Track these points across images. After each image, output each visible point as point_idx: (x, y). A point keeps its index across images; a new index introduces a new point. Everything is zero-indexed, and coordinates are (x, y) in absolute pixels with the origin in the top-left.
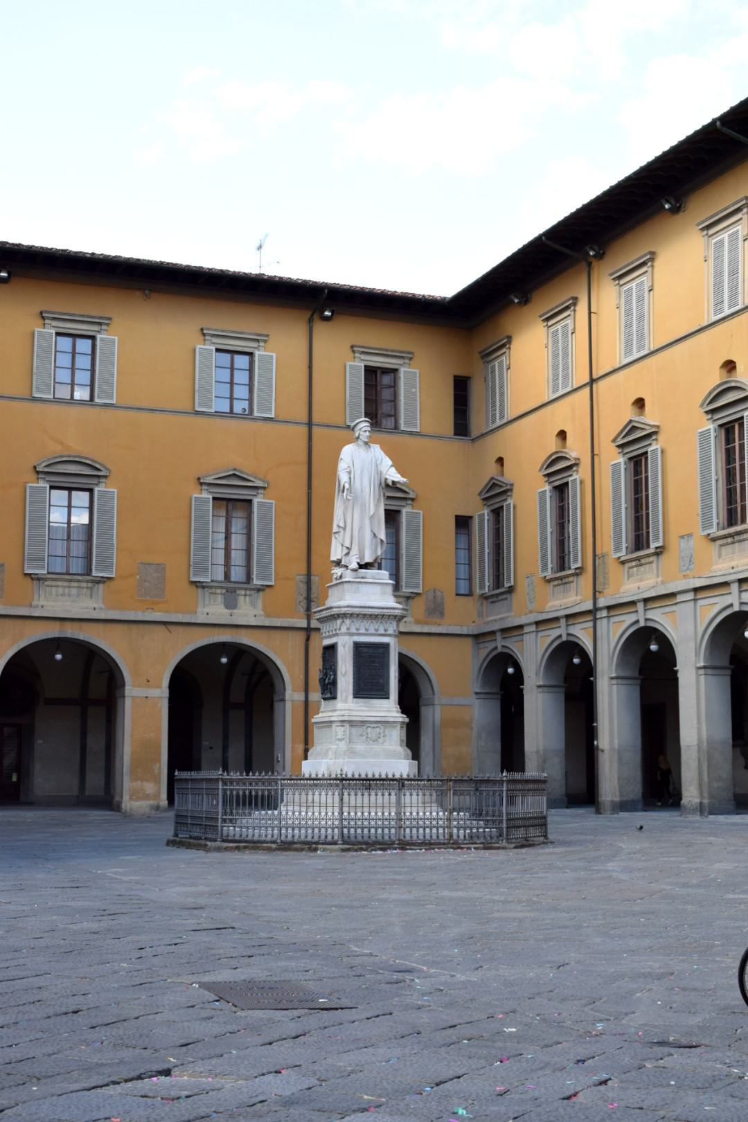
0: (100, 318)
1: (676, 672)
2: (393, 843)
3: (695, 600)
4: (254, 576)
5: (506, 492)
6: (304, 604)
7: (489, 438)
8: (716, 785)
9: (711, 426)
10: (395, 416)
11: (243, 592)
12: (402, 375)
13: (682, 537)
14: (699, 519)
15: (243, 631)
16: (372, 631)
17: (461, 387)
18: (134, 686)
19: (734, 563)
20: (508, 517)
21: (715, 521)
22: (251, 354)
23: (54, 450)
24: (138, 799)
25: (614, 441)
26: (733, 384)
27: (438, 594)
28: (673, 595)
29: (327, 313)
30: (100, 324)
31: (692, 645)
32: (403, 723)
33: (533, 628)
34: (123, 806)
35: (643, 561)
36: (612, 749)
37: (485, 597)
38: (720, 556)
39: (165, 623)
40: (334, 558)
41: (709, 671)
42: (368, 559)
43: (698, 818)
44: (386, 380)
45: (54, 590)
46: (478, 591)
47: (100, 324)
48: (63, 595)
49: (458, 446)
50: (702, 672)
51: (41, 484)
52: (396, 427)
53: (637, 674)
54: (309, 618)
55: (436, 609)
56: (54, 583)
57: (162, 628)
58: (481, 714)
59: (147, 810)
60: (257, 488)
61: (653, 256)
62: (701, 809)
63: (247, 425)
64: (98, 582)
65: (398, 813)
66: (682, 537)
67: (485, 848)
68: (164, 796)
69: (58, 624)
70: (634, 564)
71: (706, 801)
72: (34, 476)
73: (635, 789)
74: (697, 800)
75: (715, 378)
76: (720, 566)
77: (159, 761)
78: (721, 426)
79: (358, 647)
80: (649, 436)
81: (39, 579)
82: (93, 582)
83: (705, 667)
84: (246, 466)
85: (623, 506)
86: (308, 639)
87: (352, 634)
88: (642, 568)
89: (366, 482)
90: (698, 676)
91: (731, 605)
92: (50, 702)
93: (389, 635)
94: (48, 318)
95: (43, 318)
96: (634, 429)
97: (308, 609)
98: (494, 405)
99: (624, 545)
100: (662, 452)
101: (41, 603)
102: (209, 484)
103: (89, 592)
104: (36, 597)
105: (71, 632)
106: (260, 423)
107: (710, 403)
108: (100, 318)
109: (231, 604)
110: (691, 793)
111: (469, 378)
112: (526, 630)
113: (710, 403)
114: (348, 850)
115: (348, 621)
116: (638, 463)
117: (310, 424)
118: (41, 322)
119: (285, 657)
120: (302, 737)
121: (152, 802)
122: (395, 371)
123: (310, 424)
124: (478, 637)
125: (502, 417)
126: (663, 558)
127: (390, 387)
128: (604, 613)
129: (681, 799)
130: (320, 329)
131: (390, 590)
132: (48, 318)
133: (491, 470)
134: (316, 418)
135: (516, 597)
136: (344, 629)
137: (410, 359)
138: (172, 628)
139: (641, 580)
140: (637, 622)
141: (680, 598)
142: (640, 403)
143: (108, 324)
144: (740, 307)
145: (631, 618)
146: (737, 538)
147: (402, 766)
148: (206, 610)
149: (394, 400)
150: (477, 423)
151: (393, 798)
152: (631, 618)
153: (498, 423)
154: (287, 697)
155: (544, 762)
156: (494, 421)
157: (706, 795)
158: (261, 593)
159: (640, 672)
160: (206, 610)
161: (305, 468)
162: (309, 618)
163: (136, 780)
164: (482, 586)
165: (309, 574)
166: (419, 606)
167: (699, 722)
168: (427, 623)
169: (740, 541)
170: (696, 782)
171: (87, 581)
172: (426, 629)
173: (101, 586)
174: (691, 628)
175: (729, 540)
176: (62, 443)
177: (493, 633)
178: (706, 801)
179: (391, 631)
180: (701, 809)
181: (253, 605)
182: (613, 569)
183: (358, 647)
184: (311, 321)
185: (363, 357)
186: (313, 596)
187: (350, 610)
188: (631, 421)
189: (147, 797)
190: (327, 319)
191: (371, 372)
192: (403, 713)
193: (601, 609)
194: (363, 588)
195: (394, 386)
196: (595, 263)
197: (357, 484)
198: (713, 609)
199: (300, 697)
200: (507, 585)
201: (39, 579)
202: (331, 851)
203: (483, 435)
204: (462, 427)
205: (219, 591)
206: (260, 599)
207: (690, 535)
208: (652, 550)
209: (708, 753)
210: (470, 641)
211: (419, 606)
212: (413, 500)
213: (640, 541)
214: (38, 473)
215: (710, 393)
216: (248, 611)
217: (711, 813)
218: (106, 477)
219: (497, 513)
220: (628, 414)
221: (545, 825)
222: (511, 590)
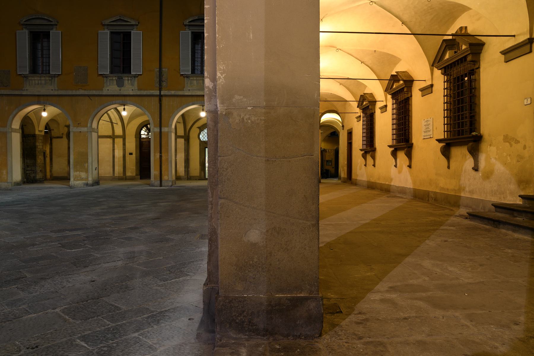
11: (127, 78)
18: (74, 126)
24: (78, 180)
39: (89, 96)
48: (38, 84)
54: (160, 90)
59: (82, 185)
64: (54, 77)
77: (87, 162)
86: (160, 101)
97: (160, 85)
102: (108, 25)
109: (120, 84)
158: (136, 79)
162: (160, 90)
163: (77, 171)
173: (56, 79)
189: (82, 179)
205: (114, 78)
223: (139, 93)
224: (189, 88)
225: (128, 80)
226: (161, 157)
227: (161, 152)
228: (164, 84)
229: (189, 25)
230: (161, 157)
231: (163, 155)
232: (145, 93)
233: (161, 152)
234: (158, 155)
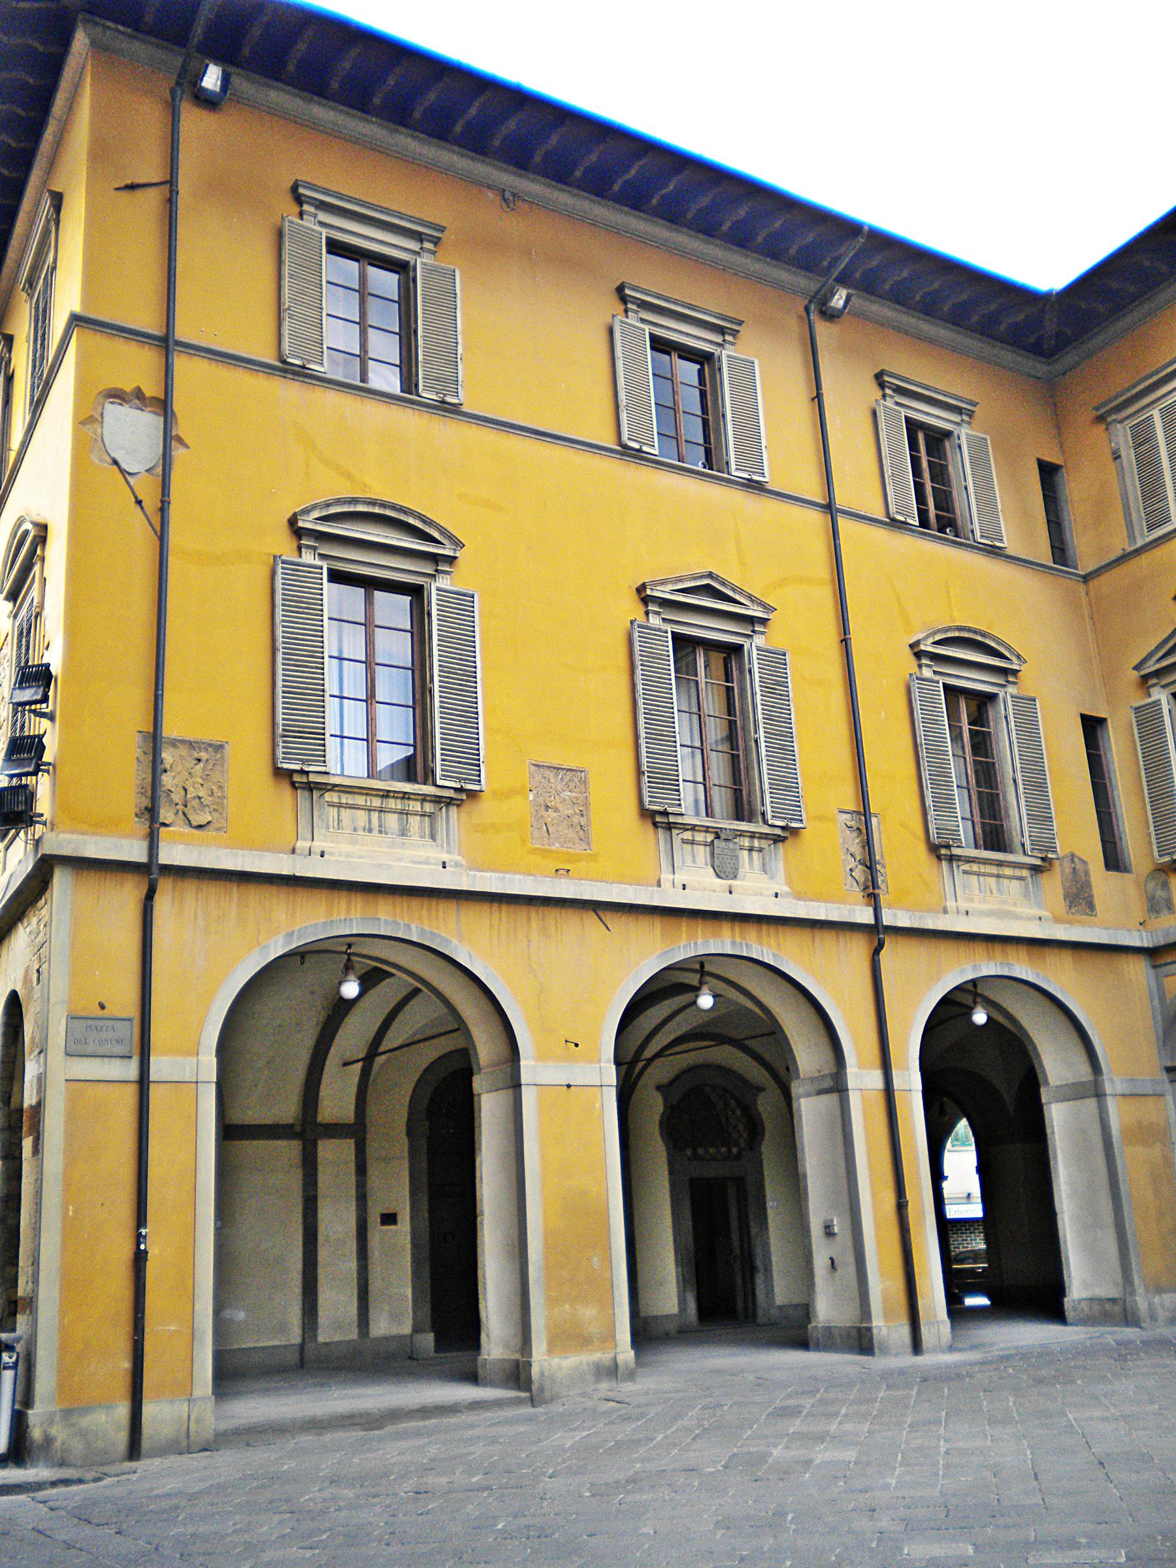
11: (746, 842)
15: (752, 932)
23: (330, 486)
27: (1079, 866)
34: (535, 1371)
51: (308, 558)
55: (1080, 898)
56: (345, 799)
57: (590, 918)
60: (751, 620)
64: (449, 802)
68: (624, 1334)
81: (310, 787)
84: (730, 573)
101: (318, 845)
102: (665, 603)
106: (737, 497)
111: (1060, 467)
118: (296, 209)
121: (597, 1356)
138: (609, 918)
148: (680, 878)
154: (851, 1083)
160: (680, 878)
161: (825, 596)
165: (865, 812)
173: (453, 811)
176: (348, 476)
191: (913, 427)
199: (875, 1079)
205: (700, 837)
211: (1054, 885)
216: (758, 888)
218: (451, 560)
224: (964, 905)
225: (751, 849)
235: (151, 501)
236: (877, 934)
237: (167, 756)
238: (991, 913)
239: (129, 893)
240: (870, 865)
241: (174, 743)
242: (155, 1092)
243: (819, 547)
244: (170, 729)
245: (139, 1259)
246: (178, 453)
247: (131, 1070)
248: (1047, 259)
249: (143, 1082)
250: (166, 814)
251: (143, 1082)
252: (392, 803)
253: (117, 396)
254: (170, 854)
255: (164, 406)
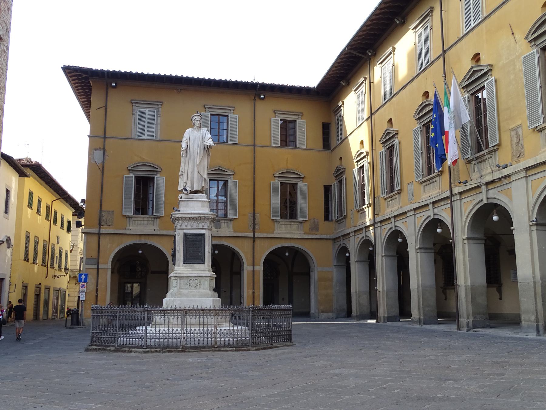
0: (157, 102)
1: (408, 251)
2: (179, 348)
3: (415, 215)
4: (229, 214)
5: (343, 172)
6: (252, 226)
7: (337, 149)
8: (427, 309)
9: (419, 126)
10: (295, 141)
11: (223, 221)
12: (298, 123)
13: (409, 184)
14: (415, 173)
15: (224, 239)
16: (195, 227)
17: (326, 129)
19: (430, 194)
20: (344, 182)
21: (421, 174)
22: (227, 116)
25: (380, 141)
26: (427, 103)
27: (316, 220)
28: (405, 213)
29: (262, 96)
30: (158, 105)
31: (414, 237)
32: (211, 278)
33: (353, 234)
35: (393, 198)
36: (383, 290)
37: (337, 221)
38: (424, 191)
40: (179, 189)
41: (422, 251)
42: (195, 188)
43: (418, 326)
44: (291, 125)
45: (136, 222)
46: (334, 219)
47: (158, 105)
49: (325, 153)
50: (418, 251)
51: (131, 175)
52: (296, 146)
53: (395, 254)
55: (315, 228)
56: (136, 219)
58: (336, 274)
60: (230, 175)
61: (394, 50)
62: (419, 321)
63: (225, 147)
64: (157, 218)
65: (182, 329)
66: (409, 184)
67: (235, 351)
69: (138, 237)
70: (390, 199)
71: (422, 317)
72: (128, 172)
73: (396, 311)
74: (418, 317)
75: (419, 101)
76: (424, 196)
78: (423, 125)
79: (186, 235)
80: (394, 136)
81: (129, 217)
82: (154, 218)
83: (420, 249)
85: (385, 172)
87: (183, 229)
88: (393, 201)
89: (196, 147)
90: (417, 253)
91: (430, 216)
92: (153, 272)
93: (205, 229)
94: (134, 103)
95: (132, 103)
96: (388, 133)
97: (254, 228)
98: (338, 134)
99: (385, 191)
100: (399, 143)
101: (130, 228)
103: (152, 222)
104: (128, 225)
105: (144, 240)
106: (231, 147)
107: (418, 114)
108: (157, 102)
109: (218, 227)
110: (415, 313)
112: (351, 235)
113: (418, 114)
114: (148, 352)
115: (180, 222)
116: (390, 150)
117: (254, 146)
118: (131, 105)
119: (243, 250)
120: (252, 287)
122: (295, 121)
123: (254, 146)
124: (335, 240)
125: (341, 138)
126: (402, 194)
127: (293, 129)
128: (379, 224)
129: (411, 316)
130: (259, 104)
131: (207, 204)
132: (134, 103)
133: (337, 163)
134: (257, 143)
135: (348, 220)
136: (178, 226)
137: (302, 116)
139: (393, 207)
140: (392, 228)
141: (408, 214)
142: (390, 121)
143: (161, 105)
144: (430, 62)
145: (389, 226)
146: (431, 181)
147: (211, 301)
149: (295, 135)
150: (333, 143)
151: (180, 321)
152: (389, 226)
153: (340, 141)
155: (359, 297)
156: (338, 141)
157: (422, 314)
158: (232, 222)
159: (397, 253)
164: (335, 217)
165: (254, 213)
166: (307, 226)
167: (418, 276)
168: (310, 234)
169: (433, 183)
170: (417, 307)
171: (151, 218)
172: (310, 237)
173: (158, 220)
174: (413, 229)
175: (428, 182)
176: (140, 157)
177: (339, 237)
178: (422, 317)
179: (206, 227)
180: (419, 321)
181: (228, 227)
182: (382, 201)
183: (186, 235)
184: (254, 100)
185: (279, 115)
186: (256, 223)
187: (180, 215)
188: (386, 130)
190: (262, 99)
192: (213, 272)
193: (377, 223)
194: (191, 204)
195: (294, 128)
196: (372, 60)
197: (191, 149)
198: (423, 218)
199: (251, 268)
200: (343, 215)
201: (129, 217)
202: (139, 352)
203: (335, 148)
204: (326, 144)
206: (231, 224)
207: (412, 182)
208: (396, 192)
209: (424, 291)
210: (331, 242)
212: (303, 178)
213: (392, 189)
214: (129, 170)
215: (417, 110)
217: (425, 323)
218: (160, 171)
219: (340, 182)
220: (386, 126)
221: (290, 335)
222: (345, 217)
223: (235, 235)
224: (279, 232)
226: (254, 293)
227: (254, 289)
228: (257, 227)
229: (278, 177)
230: (254, 293)
231: (256, 291)
232: (240, 235)
233: (254, 289)
234: (251, 292)
235: (101, 168)
236: (254, 238)
237: (103, 213)
238: (287, 233)
239: (96, 238)
240: (254, 224)
241: (105, 211)
242: (100, 270)
243: (251, 155)
244: (103, 210)
245: (97, 296)
246: (106, 157)
247: (96, 267)
248: (312, 80)
249: (98, 269)
250: (102, 224)
251: (98, 269)
252: (145, 219)
253: (96, 149)
254: (103, 231)
255: (104, 150)
